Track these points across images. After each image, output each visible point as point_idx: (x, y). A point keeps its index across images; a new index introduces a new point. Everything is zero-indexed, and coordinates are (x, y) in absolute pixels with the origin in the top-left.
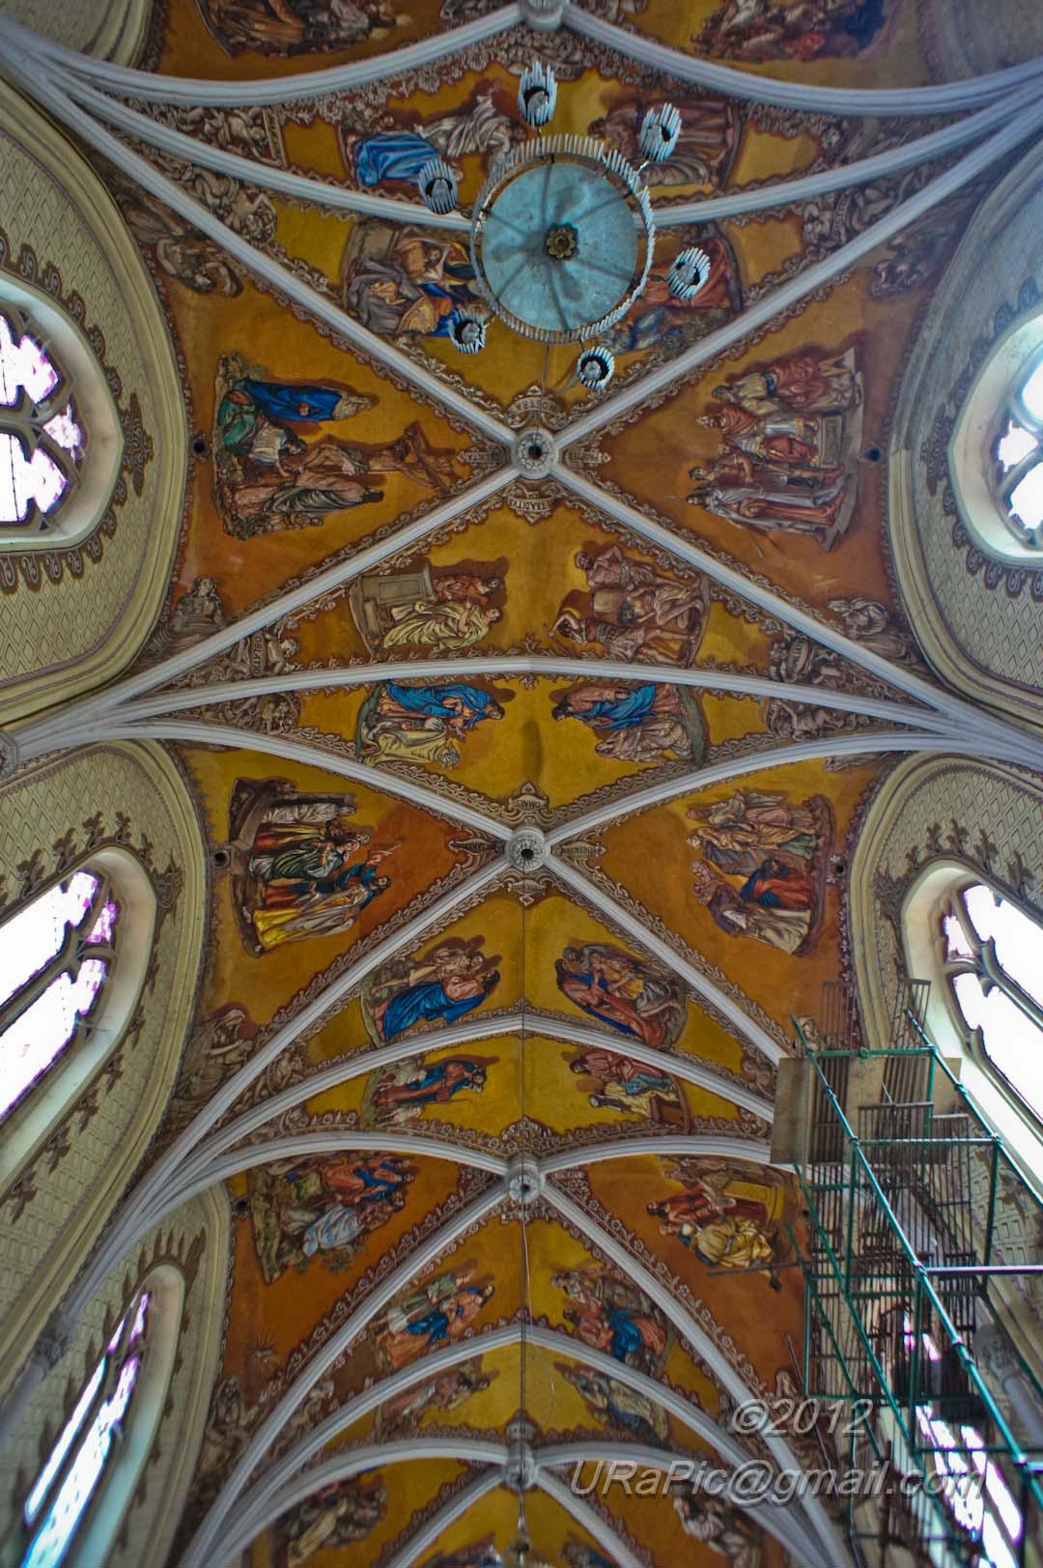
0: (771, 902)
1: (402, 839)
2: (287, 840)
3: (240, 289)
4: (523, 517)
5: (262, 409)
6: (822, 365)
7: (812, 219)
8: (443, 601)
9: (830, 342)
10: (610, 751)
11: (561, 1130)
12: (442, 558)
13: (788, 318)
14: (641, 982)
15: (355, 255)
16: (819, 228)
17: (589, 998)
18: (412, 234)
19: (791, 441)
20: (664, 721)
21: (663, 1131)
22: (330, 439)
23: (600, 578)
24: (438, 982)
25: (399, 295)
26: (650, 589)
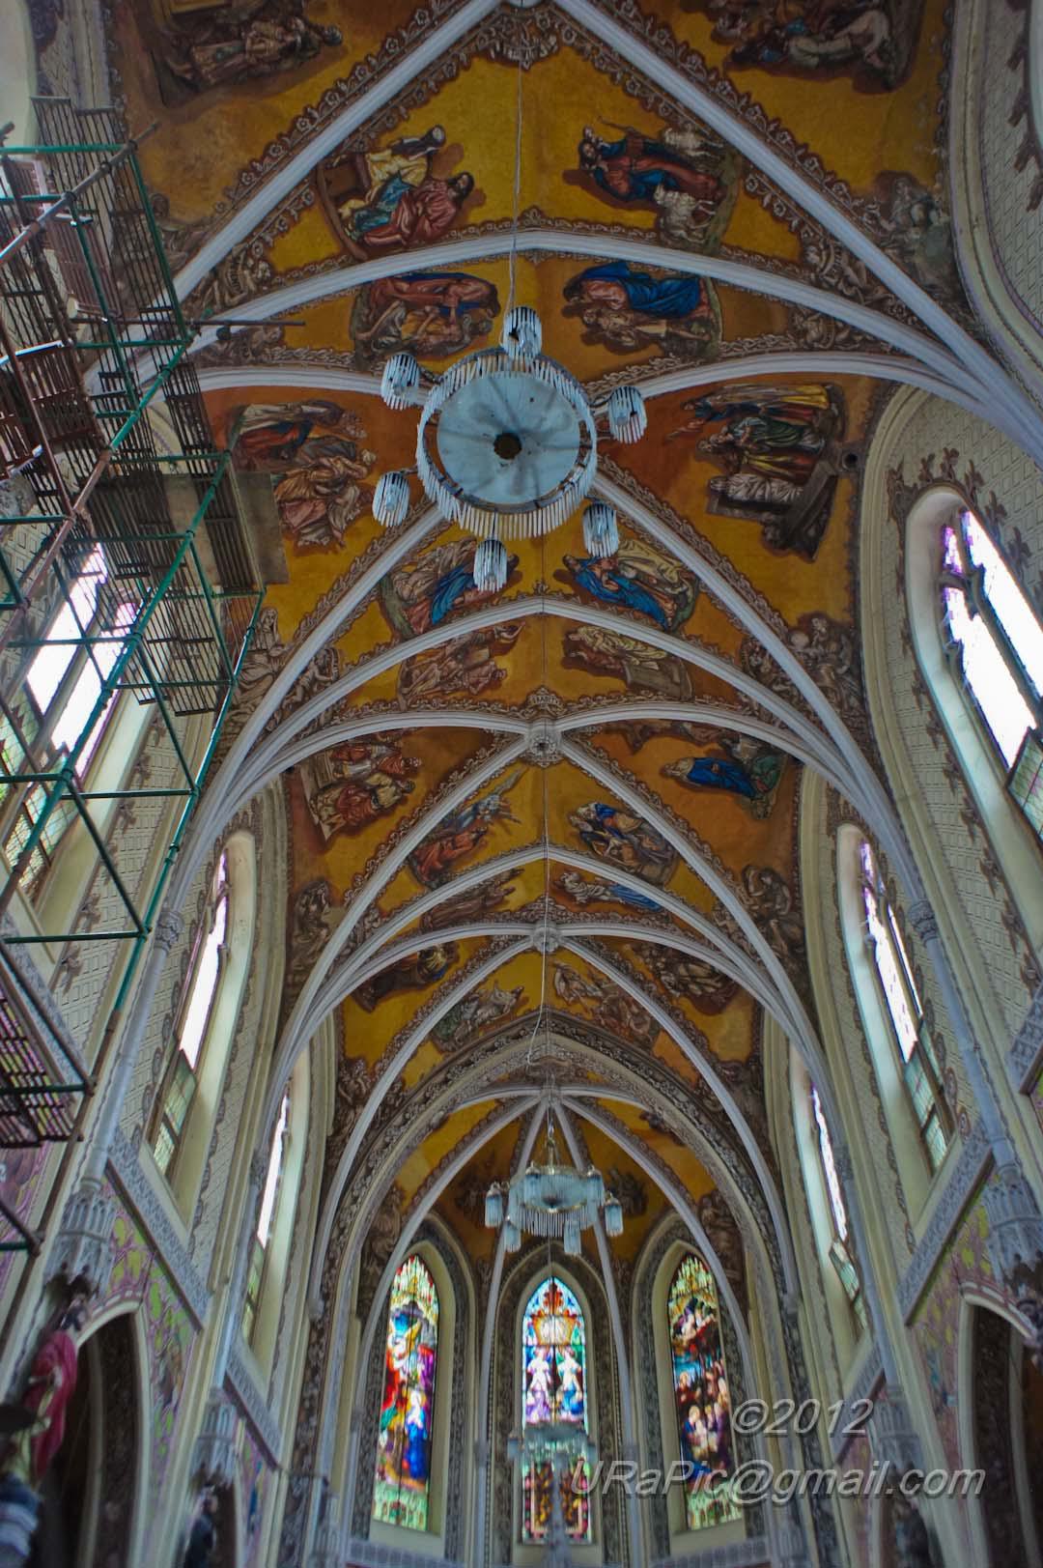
0: (283, 427)
1: (665, 443)
2: (781, 459)
3: (744, 872)
4: (550, 692)
5: (746, 775)
6: (342, 822)
7: (376, 920)
8: (615, 657)
9: (342, 840)
10: (464, 545)
11: (476, 61)
12: (616, 684)
13: (375, 857)
14: (405, 335)
15: (667, 870)
16: (371, 918)
17: (459, 290)
18: (630, 868)
19: (350, 759)
20: (419, 596)
21: (348, 143)
22: (699, 744)
23: (486, 668)
24: (635, 310)
25: (641, 839)
26: (445, 680)
